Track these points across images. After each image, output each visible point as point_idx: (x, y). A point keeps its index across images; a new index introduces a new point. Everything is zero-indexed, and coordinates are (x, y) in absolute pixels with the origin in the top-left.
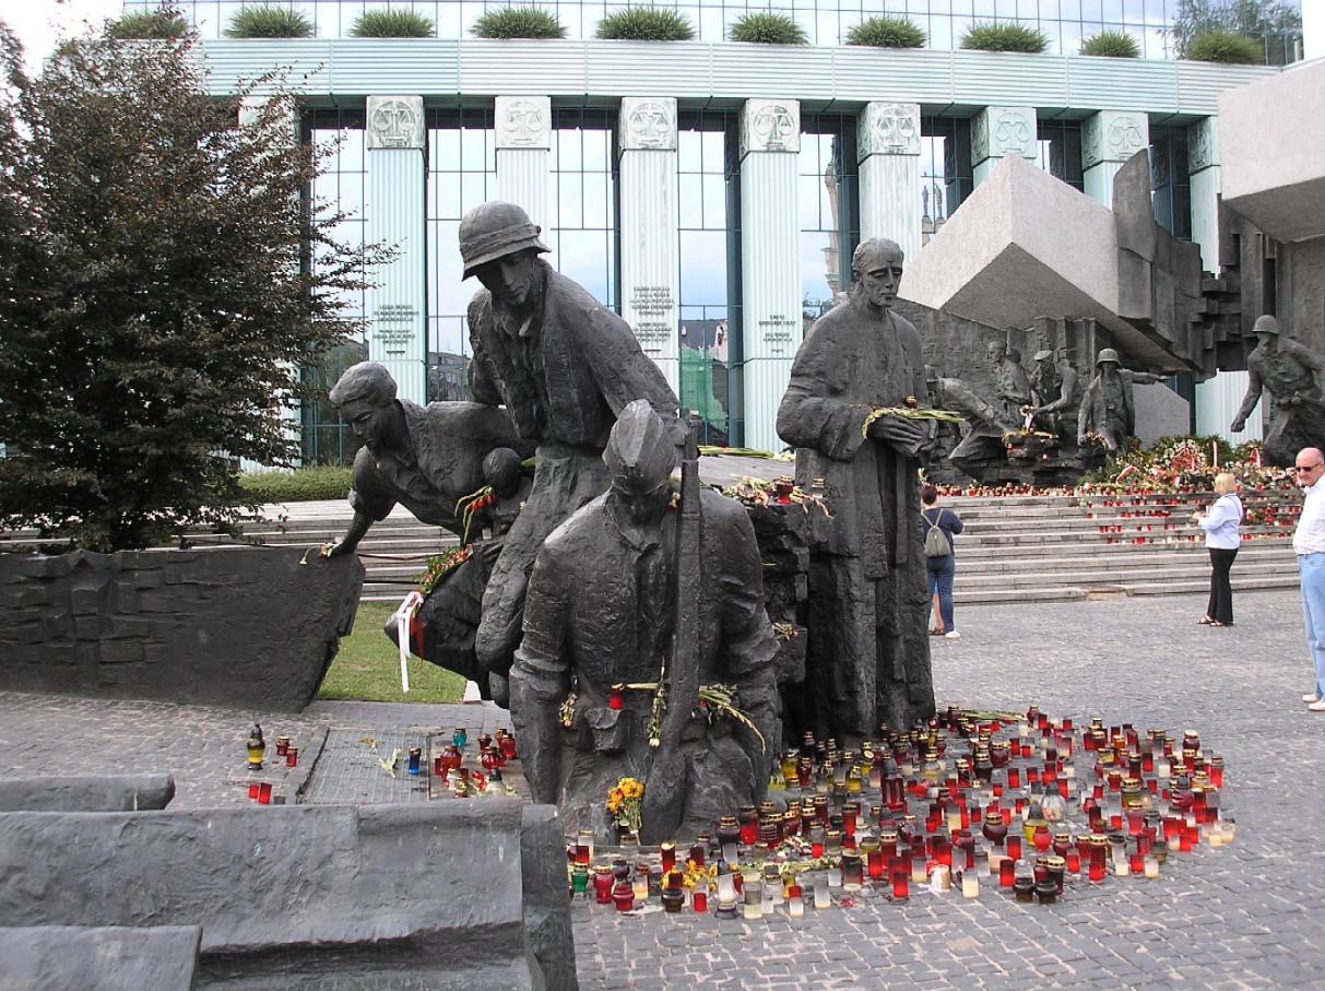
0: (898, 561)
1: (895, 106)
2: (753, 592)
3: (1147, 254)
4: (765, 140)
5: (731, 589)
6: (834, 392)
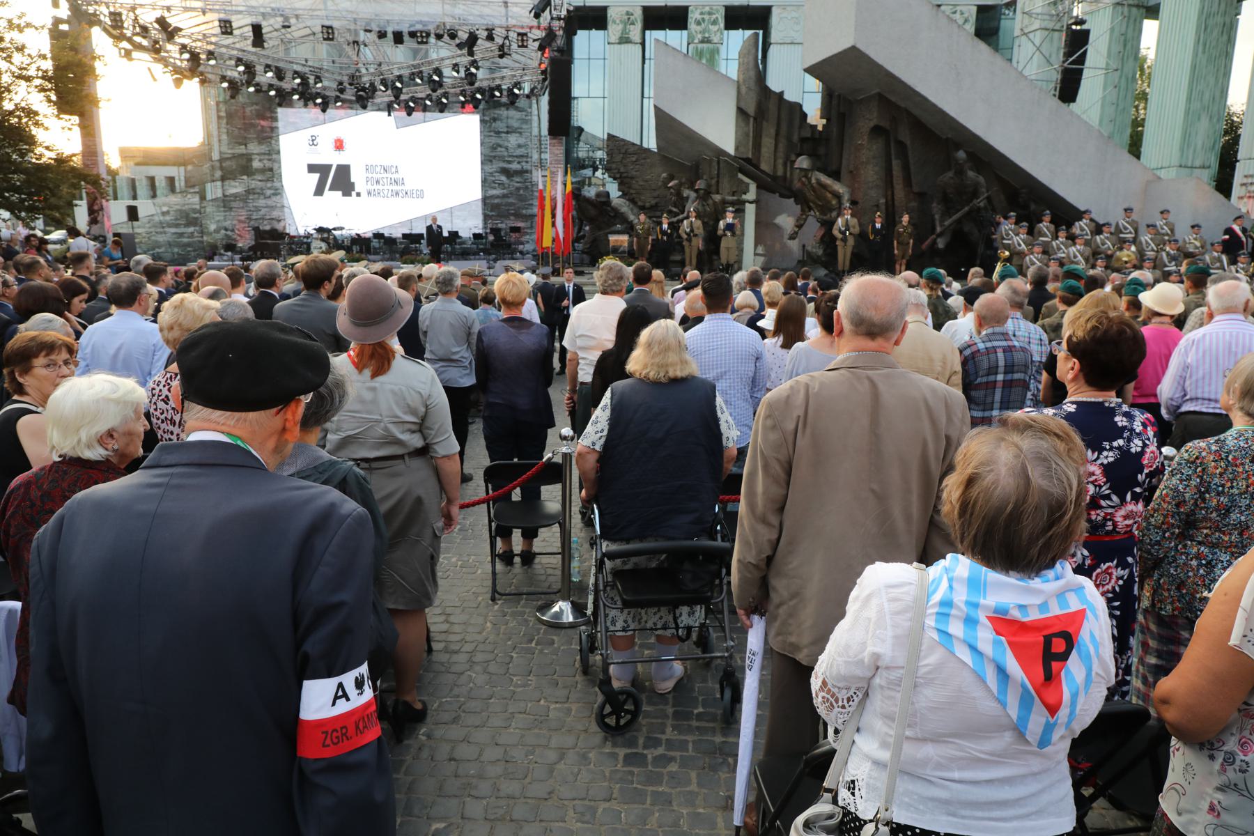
1: (707, 9)
3: (751, 110)
4: (618, 35)
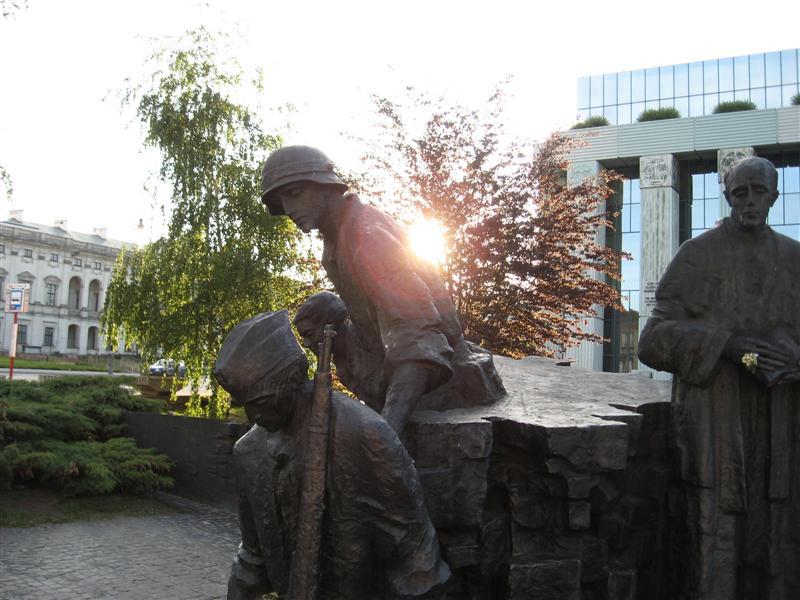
0: (773, 495)
2: (398, 518)
5: (375, 512)
6: (692, 315)
